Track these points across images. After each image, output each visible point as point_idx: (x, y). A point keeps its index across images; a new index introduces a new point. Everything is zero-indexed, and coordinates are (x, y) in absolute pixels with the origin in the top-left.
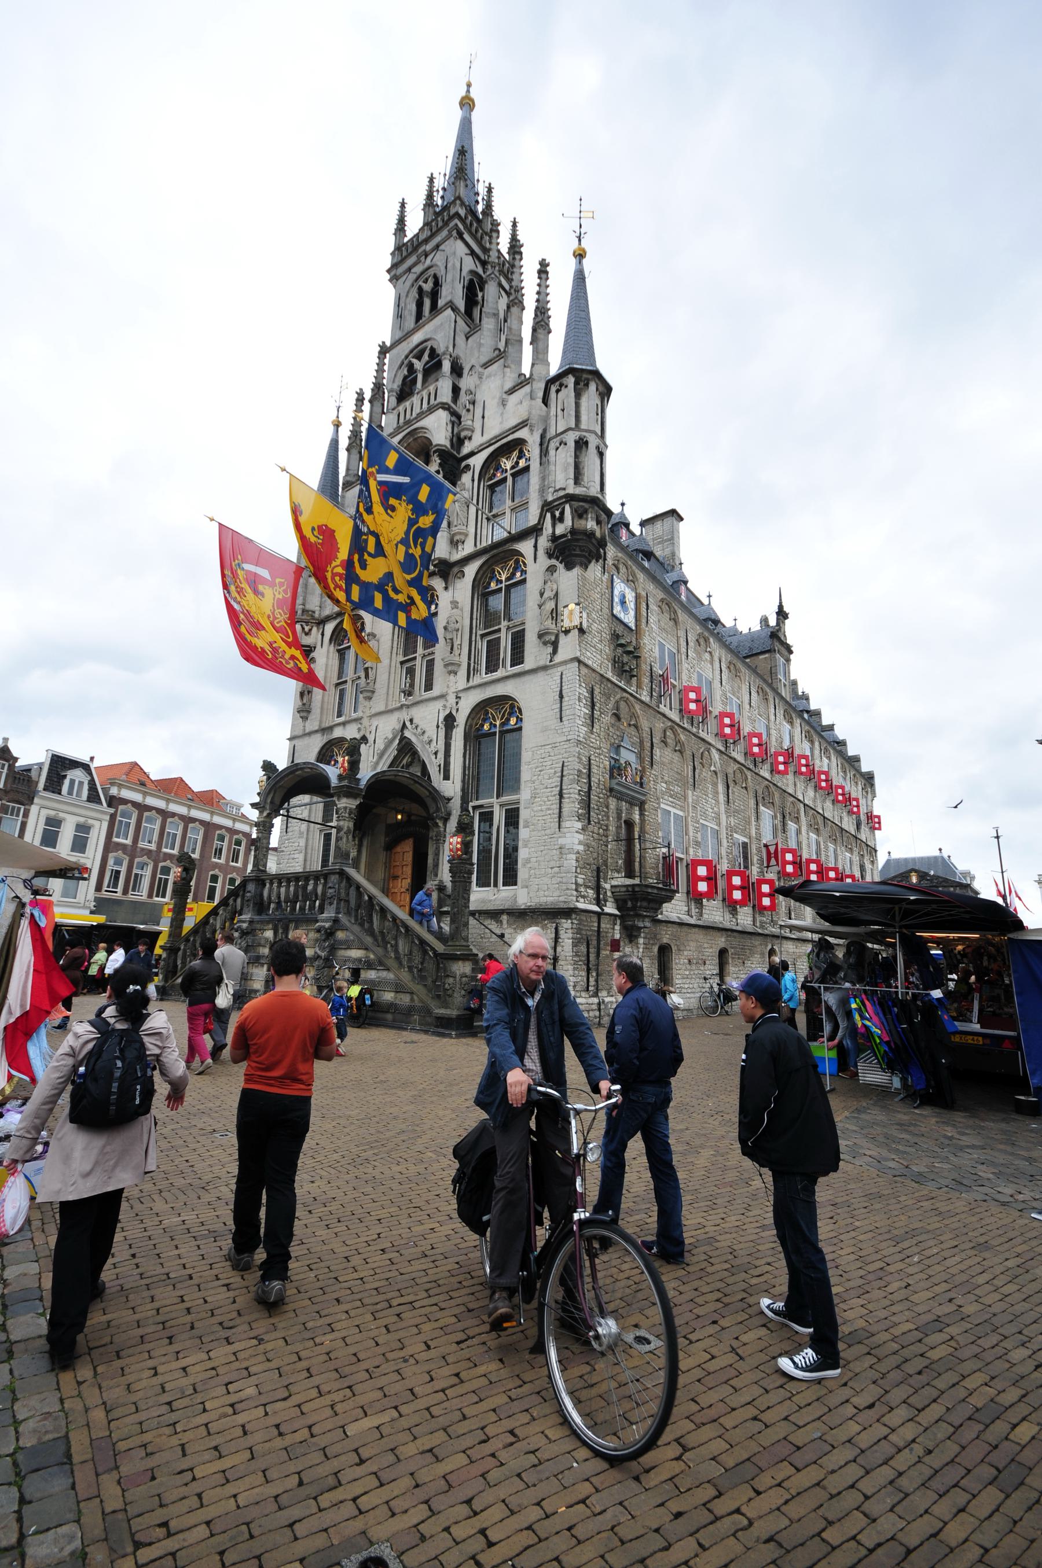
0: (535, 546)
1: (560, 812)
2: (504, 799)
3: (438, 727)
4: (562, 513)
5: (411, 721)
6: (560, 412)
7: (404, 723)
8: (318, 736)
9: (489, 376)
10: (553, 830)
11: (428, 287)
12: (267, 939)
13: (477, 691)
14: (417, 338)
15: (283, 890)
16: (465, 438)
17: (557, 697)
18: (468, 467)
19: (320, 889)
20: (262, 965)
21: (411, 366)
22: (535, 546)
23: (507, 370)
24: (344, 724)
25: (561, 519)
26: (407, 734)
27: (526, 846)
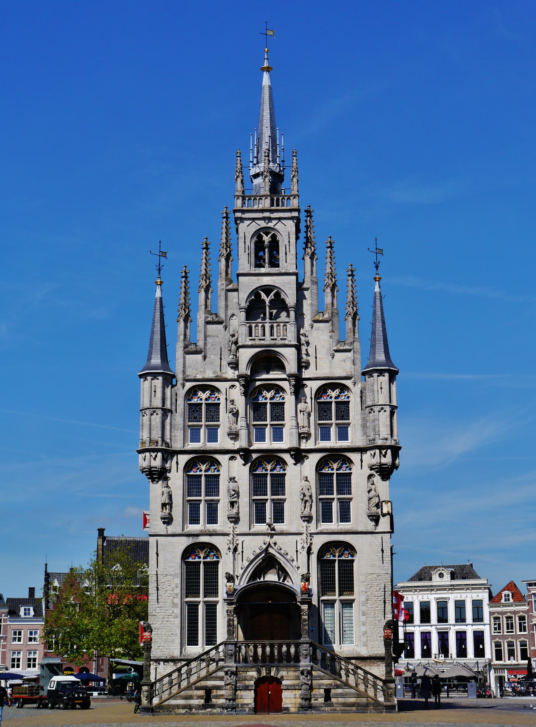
0: (361, 460)
1: (385, 610)
2: (342, 598)
3: (297, 551)
4: (386, 453)
5: (275, 544)
6: (380, 389)
7: (269, 544)
8: (184, 538)
9: (318, 329)
10: (380, 618)
11: (266, 239)
12: (252, 677)
13: (327, 535)
14: (266, 281)
15: (260, 650)
16: (304, 366)
17: (380, 550)
18: (304, 386)
19: (292, 650)
20: (251, 690)
21: (258, 295)
22: (361, 460)
23: (334, 334)
24: (211, 535)
25: (385, 456)
26: (271, 550)
27: (364, 625)
